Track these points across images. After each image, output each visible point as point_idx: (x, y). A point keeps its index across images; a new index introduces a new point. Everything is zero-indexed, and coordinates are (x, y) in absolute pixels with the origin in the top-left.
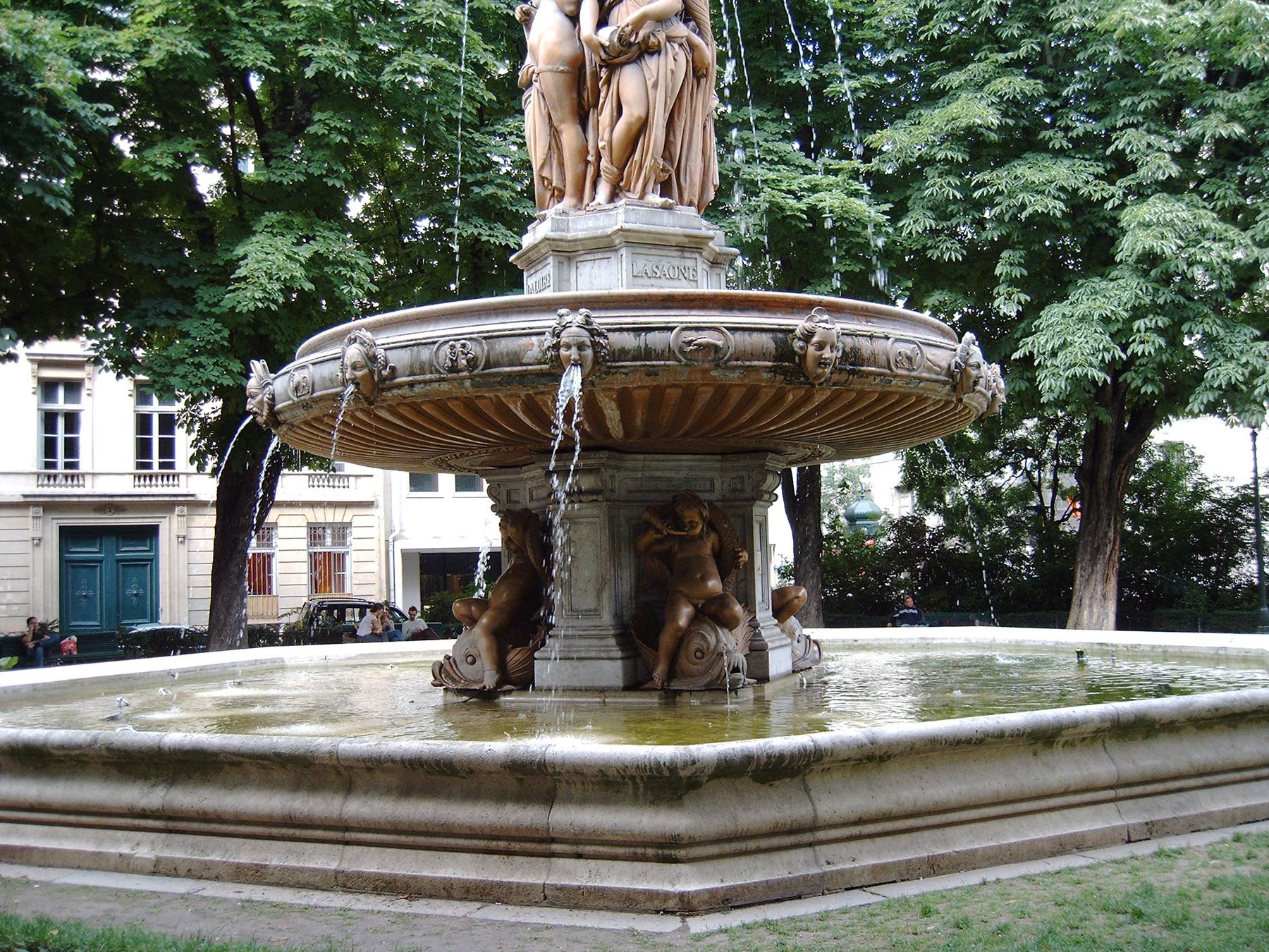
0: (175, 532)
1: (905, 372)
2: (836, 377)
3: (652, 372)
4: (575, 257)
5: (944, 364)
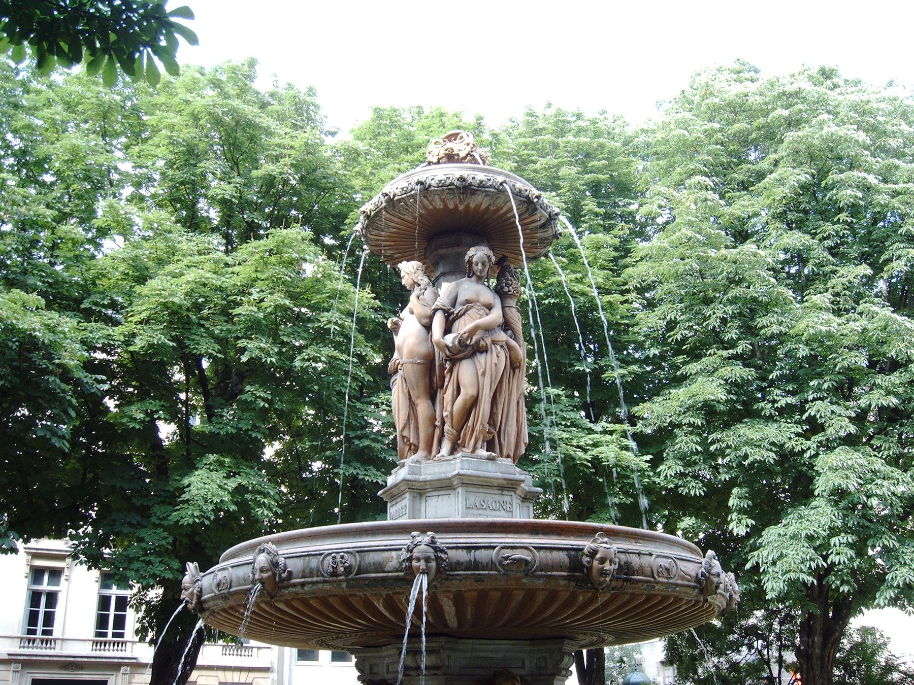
2: (614, 584)
3: (479, 579)
4: (425, 493)
5: (693, 574)
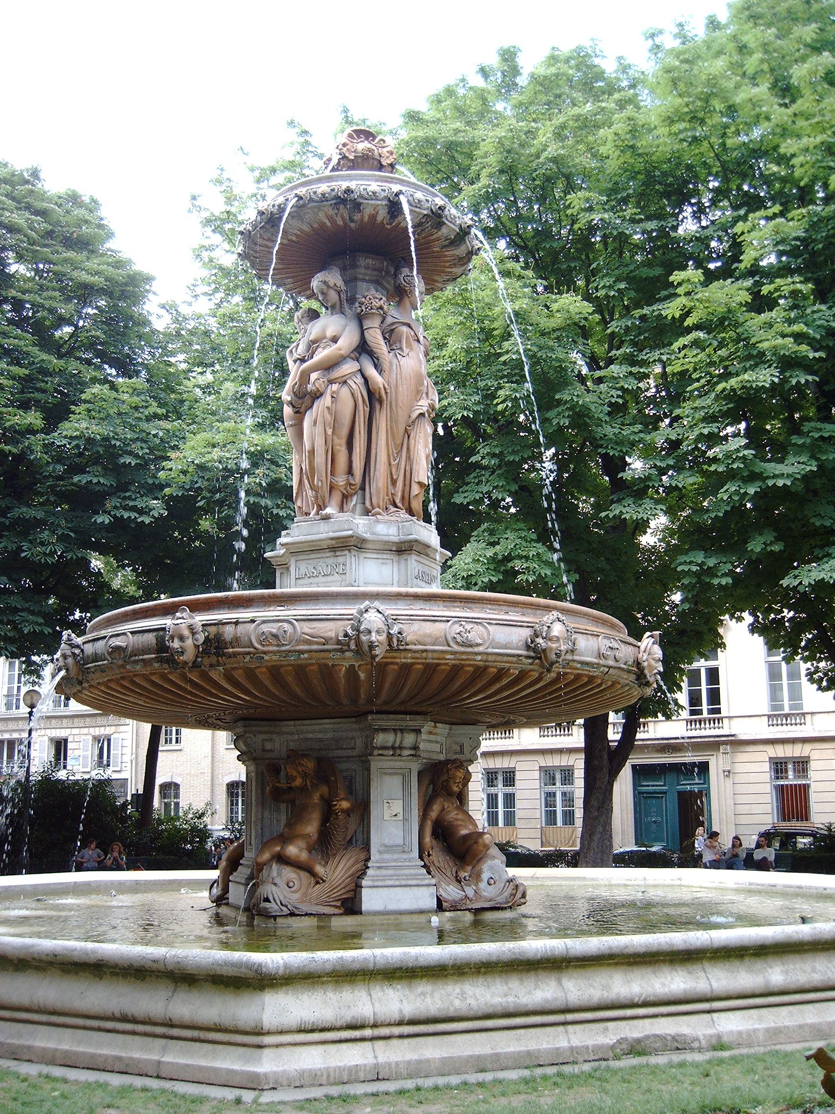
1: (271, 648)
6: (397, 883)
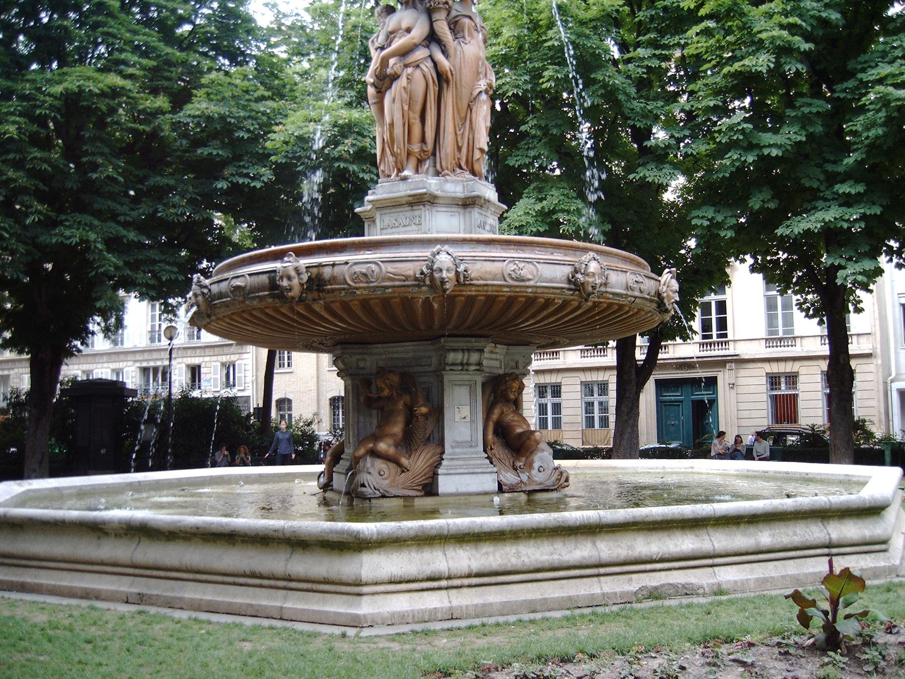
0: (728, 381)
1: (362, 285)
6: (466, 471)
